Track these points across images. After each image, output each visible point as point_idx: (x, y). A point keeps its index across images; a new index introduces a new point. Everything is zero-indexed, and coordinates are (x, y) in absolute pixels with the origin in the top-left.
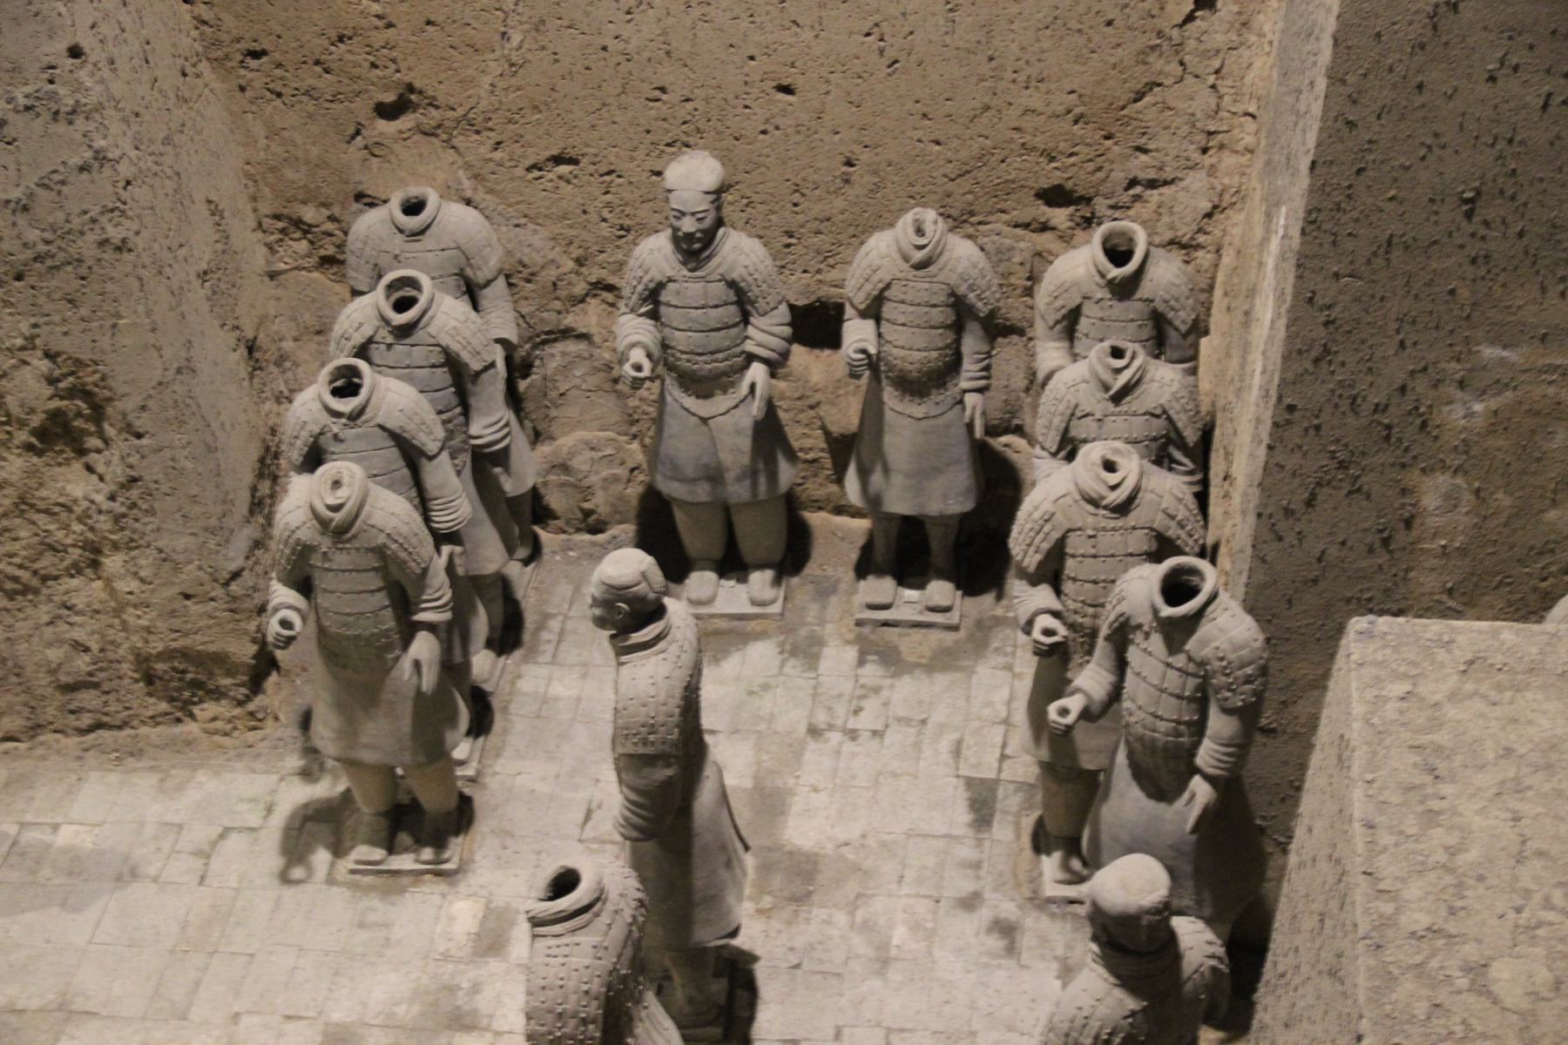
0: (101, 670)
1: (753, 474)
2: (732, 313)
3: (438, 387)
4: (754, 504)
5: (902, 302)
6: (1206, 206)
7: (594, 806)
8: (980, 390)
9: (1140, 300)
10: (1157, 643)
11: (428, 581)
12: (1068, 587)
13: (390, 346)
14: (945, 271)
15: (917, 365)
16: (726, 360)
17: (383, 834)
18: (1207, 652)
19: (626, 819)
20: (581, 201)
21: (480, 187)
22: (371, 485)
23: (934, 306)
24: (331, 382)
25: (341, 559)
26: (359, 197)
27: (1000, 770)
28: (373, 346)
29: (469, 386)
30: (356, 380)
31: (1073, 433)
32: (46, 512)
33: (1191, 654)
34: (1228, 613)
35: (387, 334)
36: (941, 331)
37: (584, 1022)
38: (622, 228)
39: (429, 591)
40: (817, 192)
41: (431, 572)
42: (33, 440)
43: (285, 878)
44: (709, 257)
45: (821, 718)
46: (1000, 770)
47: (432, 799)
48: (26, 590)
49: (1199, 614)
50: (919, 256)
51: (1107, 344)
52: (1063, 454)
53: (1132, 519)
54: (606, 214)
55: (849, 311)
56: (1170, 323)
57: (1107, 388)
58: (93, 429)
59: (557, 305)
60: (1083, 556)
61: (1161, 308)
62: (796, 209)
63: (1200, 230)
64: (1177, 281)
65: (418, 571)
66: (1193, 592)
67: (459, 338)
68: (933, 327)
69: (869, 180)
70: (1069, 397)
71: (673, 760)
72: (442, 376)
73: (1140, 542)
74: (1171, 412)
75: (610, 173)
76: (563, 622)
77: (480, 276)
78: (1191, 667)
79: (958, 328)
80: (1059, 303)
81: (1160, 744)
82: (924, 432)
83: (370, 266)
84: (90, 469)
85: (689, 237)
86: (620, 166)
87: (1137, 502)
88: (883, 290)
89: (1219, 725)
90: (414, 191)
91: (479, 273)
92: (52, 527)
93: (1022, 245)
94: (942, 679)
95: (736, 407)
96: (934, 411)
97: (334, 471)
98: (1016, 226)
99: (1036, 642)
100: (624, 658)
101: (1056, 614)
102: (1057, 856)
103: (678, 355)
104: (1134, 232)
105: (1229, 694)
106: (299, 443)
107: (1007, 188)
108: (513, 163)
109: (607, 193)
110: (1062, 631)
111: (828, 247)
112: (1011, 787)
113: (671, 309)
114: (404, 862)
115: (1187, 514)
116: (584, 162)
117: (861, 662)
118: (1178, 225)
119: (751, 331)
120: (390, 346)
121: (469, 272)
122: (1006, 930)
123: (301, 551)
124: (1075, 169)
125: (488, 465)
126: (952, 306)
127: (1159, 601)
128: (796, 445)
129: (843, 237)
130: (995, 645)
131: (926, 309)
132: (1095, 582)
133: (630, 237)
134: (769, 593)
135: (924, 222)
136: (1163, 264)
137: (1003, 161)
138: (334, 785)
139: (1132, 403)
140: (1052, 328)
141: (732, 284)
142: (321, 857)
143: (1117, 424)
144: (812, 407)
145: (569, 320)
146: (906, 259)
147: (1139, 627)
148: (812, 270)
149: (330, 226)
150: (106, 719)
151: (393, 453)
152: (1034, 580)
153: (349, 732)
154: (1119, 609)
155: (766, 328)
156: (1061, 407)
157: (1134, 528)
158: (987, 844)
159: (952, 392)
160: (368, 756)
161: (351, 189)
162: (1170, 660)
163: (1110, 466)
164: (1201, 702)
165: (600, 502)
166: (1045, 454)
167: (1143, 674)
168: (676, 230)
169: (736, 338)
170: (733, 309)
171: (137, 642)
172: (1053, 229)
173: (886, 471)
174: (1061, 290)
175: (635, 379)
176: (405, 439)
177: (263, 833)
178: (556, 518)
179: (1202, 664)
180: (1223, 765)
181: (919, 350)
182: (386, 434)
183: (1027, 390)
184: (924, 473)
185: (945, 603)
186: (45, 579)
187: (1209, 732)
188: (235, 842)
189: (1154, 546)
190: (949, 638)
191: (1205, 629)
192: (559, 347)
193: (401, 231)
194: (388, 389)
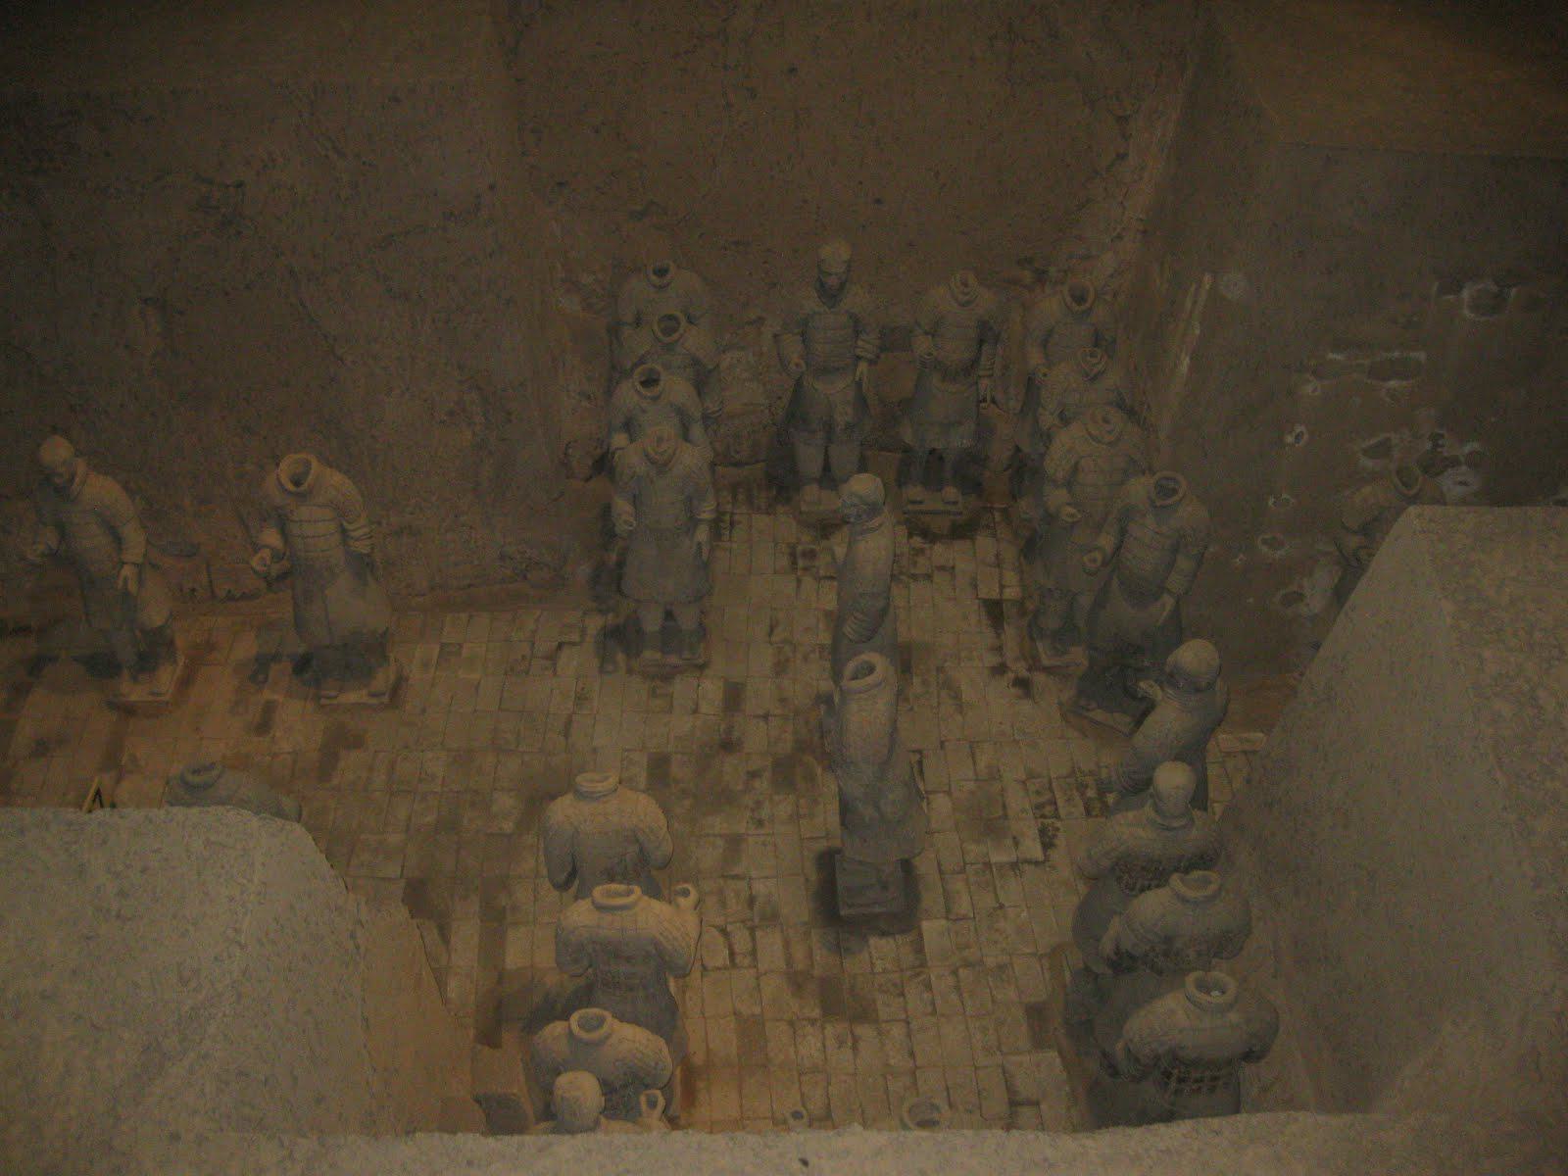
27: (1001, 593)
43: (602, 670)
46: (1001, 593)
89: (1184, 564)
94: (960, 545)
101: (1069, 504)
122: (1023, 685)
142: (621, 657)
158: (1003, 637)
188: (566, 652)
193: (654, 286)
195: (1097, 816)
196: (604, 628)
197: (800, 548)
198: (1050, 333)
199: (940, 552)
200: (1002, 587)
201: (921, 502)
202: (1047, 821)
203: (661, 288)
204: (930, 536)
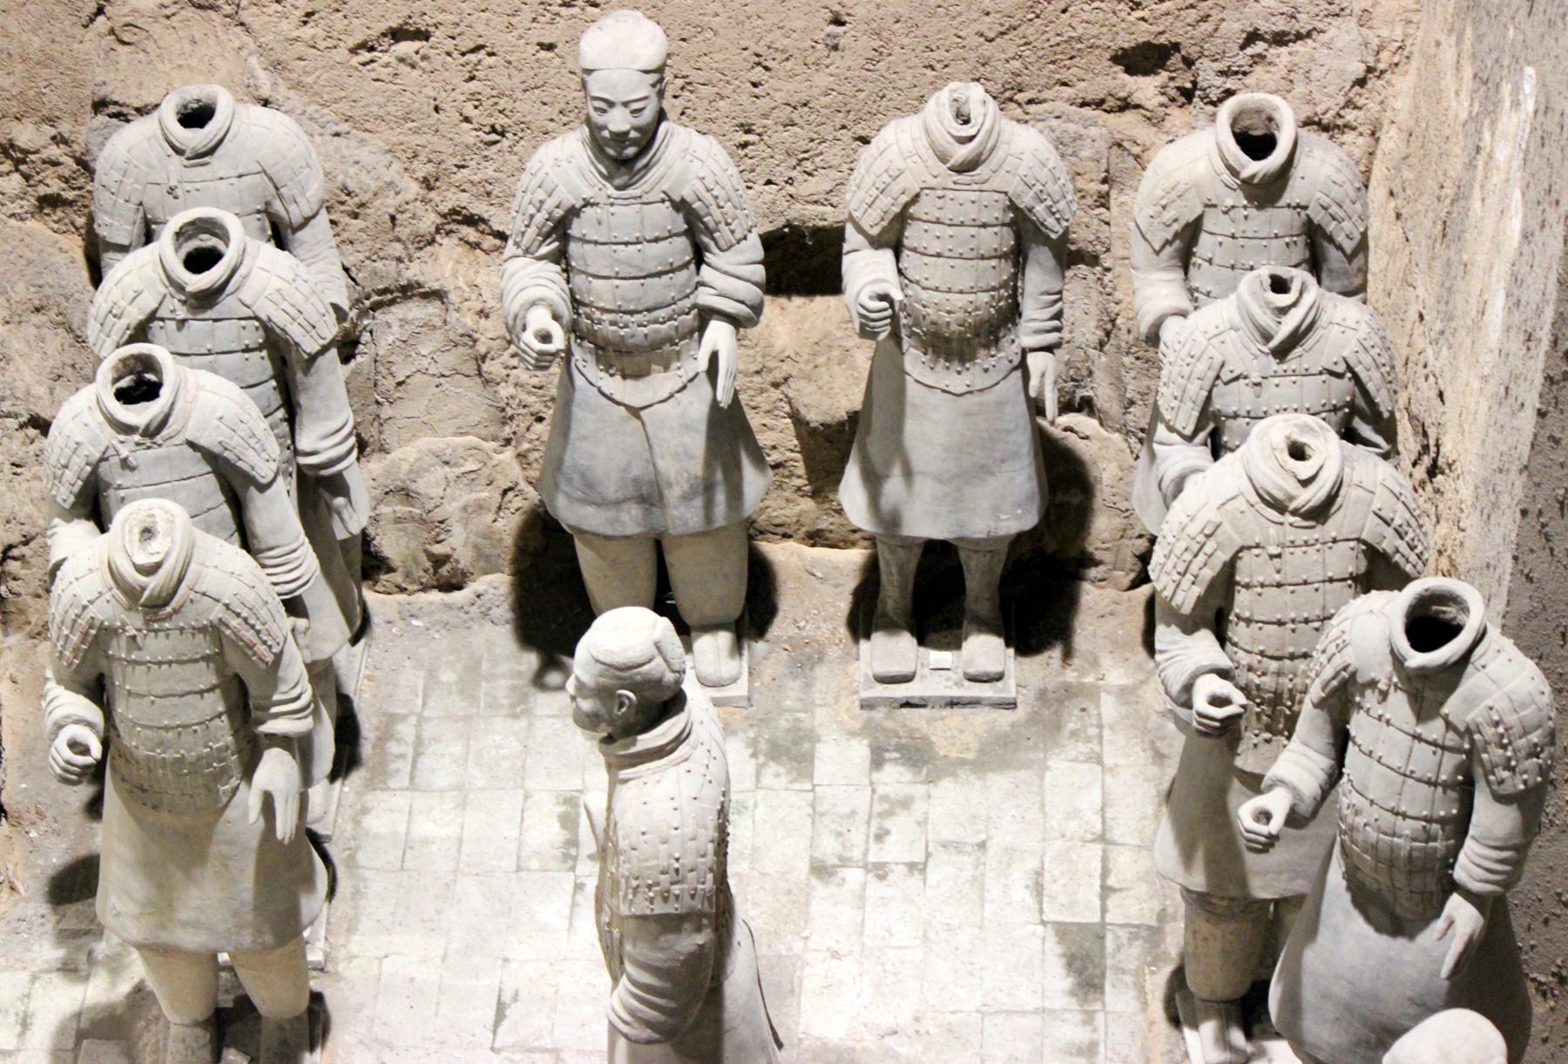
1: (708, 488)
2: (680, 248)
3: (252, 382)
4: (707, 533)
5: (938, 222)
6: (1358, 70)
7: (507, 998)
8: (1049, 349)
9: (1289, 206)
10: (1399, 706)
11: (281, 673)
12: (1237, 632)
13: (182, 323)
14: (1002, 172)
15: (960, 315)
16: (671, 318)
18: (1475, 715)
19: (632, 1012)
20: (433, 94)
21: (281, 81)
22: (200, 534)
23: (985, 226)
24: (116, 380)
25: (155, 646)
26: (100, 105)
27: (1104, 911)
28: (157, 324)
29: (299, 375)
30: (150, 377)
31: (1217, 404)
33: (1451, 718)
34: (1503, 657)
35: (178, 305)
36: (994, 262)
38: (494, 130)
39: (283, 687)
40: (789, 65)
41: (286, 658)
44: (647, 167)
45: (829, 848)
46: (1104, 911)
49: (1465, 658)
50: (962, 153)
51: (1264, 272)
53: (1332, 528)
54: (469, 110)
55: (852, 238)
56: (1331, 239)
57: (1267, 337)
59: (397, 250)
60: (1262, 585)
61: (1318, 217)
62: (756, 90)
63: (1349, 104)
64: (1339, 178)
65: (270, 658)
66: (1453, 630)
67: (285, 305)
68: (983, 258)
69: (866, 44)
70: (1211, 352)
71: (705, 921)
72: (261, 364)
73: (1347, 561)
74: (1358, 369)
75: (479, 48)
76: (419, 725)
77: (296, 214)
78: (1451, 739)
79: (1018, 257)
80: (1168, 216)
81: (1403, 853)
82: (967, 414)
83: (132, 206)
85: (621, 138)
86: (492, 38)
87: (1339, 500)
88: (907, 206)
90: (195, 92)
91: (293, 208)
93: (1093, 131)
94: (999, 782)
95: (679, 391)
96: (981, 381)
97: (143, 515)
98: (1083, 104)
99: (1200, 715)
100: (624, 774)
101: (1224, 674)
102: (1209, 1028)
103: (598, 315)
104: (1276, 109)
105: (1506, 774)
107: (1071, 50)
108: (330, 43)
109: (472, 78)
110: (1239, 698)
111: (804, 145)
112: (1123, 934)
113: (588, 247)
115: (1408, 515)
116: (438, 35)
117: (877, 762)
118: (1317, 96)
120: (182, 323)
121: (278, 207)
123: (96, 636)
124: (1170, 19)
125: (326, 495)
126: (1011, 224)
128: (764, 439)
129: (827, 131)
130: (1071, 726)
131: (973, 231)
132: (1280, 623)
133: (505, 143)
134: (728, 666)
135: (967, 101)
136: (1317, 153)
137: (1064, 11)
138: (113, 984)
139: (1299, 359)
140: (1157, 253)
141: (681, 206)
143: (1282, 389)
144: (776, 385)
145: (412, 272)
146: (943, 159)
147: (1373, 684)
148: (780, 180)
149: (55, 152)
151: (209, 484)
152: (1189, 625)
153: (161, 905)
154: (1338, 661)
156: (1201, 367)
157: (1335, 541)
158: (1100, 1017)
159: (1008, 351)
160: (189, 939)
161: (87, 94)
162: (1419, 730)
165: (458, 544)
166: (1175, 437)
167: (1377, 754)
168: (595, 129)
169: (684, 286)
170: (682, 243)
172: (1137, 107)
173: (908, 474)
174: (1174, 194)
175: (541, 353)
176: (227, 461)
177: (21, 1057)
178: (391, 570)
179: (1468, 732)
181: (961, 292)
182: (198, 455)
183: (1101, 345)
185: (994, 668)
187: (1472, 831)
189: (1363, 566)
190: (1004, 718)
191: (1471, 681)
192: (398, 311)
193: (179, 152)
194: (199, 388)
198: (1191, 232)
200: (1106, 891)
201: (906, 679)
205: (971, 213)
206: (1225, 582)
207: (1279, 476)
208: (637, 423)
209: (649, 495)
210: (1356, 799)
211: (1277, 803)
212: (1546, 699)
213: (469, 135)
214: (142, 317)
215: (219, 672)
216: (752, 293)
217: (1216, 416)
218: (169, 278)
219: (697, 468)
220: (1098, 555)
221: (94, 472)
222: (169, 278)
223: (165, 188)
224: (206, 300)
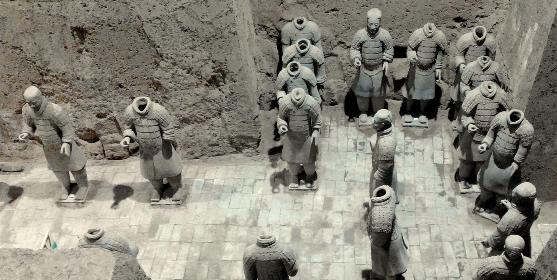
0: (220, 141)
1: (381, 90)
5: (424, 46)
7: (347, 172)
8: (440, 68)
10: (507, 130)
12: (476, 117)
17: (297, 181)
25: (298, 113)
27: (444, 162)
28: (294, 58)
29: (318, 68)
31: (472, 79)
32: (209, 101)
34: (527, 123)
35: (299, 55)
37: (389, 226)
38: (348, 28)
39: (318, 120)
42: (207, 83)
43: (273, 191)
46: (444, 162)
47: (308, 171)
48: (202, 121)
49: (520, 124)
50: (430, 35)
52: (469, 84)
54: (344, 24)
56: (490, 51)
57: (482, 68)
58: (222, 80)
59: (330, 47)
61: (488, 47)
65: (317, 115)
66: (518, 119)
69: (412, 16)
74: (497, 74)
75: (346, 14)
77: (316, 40)
78: (516, 137)
79: (437, 53)
84: (220, 90)
85: (373, 30)
88: (419, 44)
89: (521, 150)
92: (210, 105)
94: (425, 140)
98: (447, 27)
101: (474, 124)
102: (463, 182)
103: (366, 60)
106: (282, 83)
107: (445, 18)
109: (345, 18)
111: (400, 32)
114: (303, 187)
116: (340, 11)
117: (405, 136)
119: (385, 54)
120: (299, 58)
121: (313, 39)
122: (452, 201)
124: (464, 13)
127: (509, 120)
132: (484, 116)
138: (280, 169)
139: (486, 72)
141: (382, 42)
142: (281, 186)
143: (483, 77)
144: (391, 73)
147: (503, 127)
149: (273, 27)
150: (220, 153)
151: (305, 86)
153: (294, 156)
154: (497, 123)
155: (390, 53)
157: (494, 103)
158: (444, 180)
159: (433, 69)
160: (297, 161)
161: (279, 18)
162: (511, 135)
163: (489, 87)
164: (517, 145)
165: (336, 98)
166: (464, 84)
170: (381, 48)
171: (229, 133)
172: (456, 28)
173: (414, 89)
179: (519, 136)
180: (520, 159)
183: (446, 68)
184: (424, 89)
186: (207, 118)
188: (258, 183)
191: (521, 127)
193: (297, 28)
194: (305, 70)
195: (483, 258)
196: (274, 174)
197: (358, 141)
198: (466, 50)
199: (418, 144)
200: (444, 159)
201: (410, 122)
202: (461, 259)
203: (302, 29)
204: (416, 137)
205: (430, 45)
206: (475, 109)
207: (485, 92)
208: (370, 78)
209: (371, 90)
210: (498, 146)
211: (485, 146)
212: (533, 131)
213: (344, 28)
214: (292, 57)
215: (308, 117)
216: (392, 57)
217: (472, 81)
218: (297, 50)
219: (379, 86)
220: (442, 103)
221: (286, 83)
222: (297, 50)
223: (294, 35)
224: (303, 55)
